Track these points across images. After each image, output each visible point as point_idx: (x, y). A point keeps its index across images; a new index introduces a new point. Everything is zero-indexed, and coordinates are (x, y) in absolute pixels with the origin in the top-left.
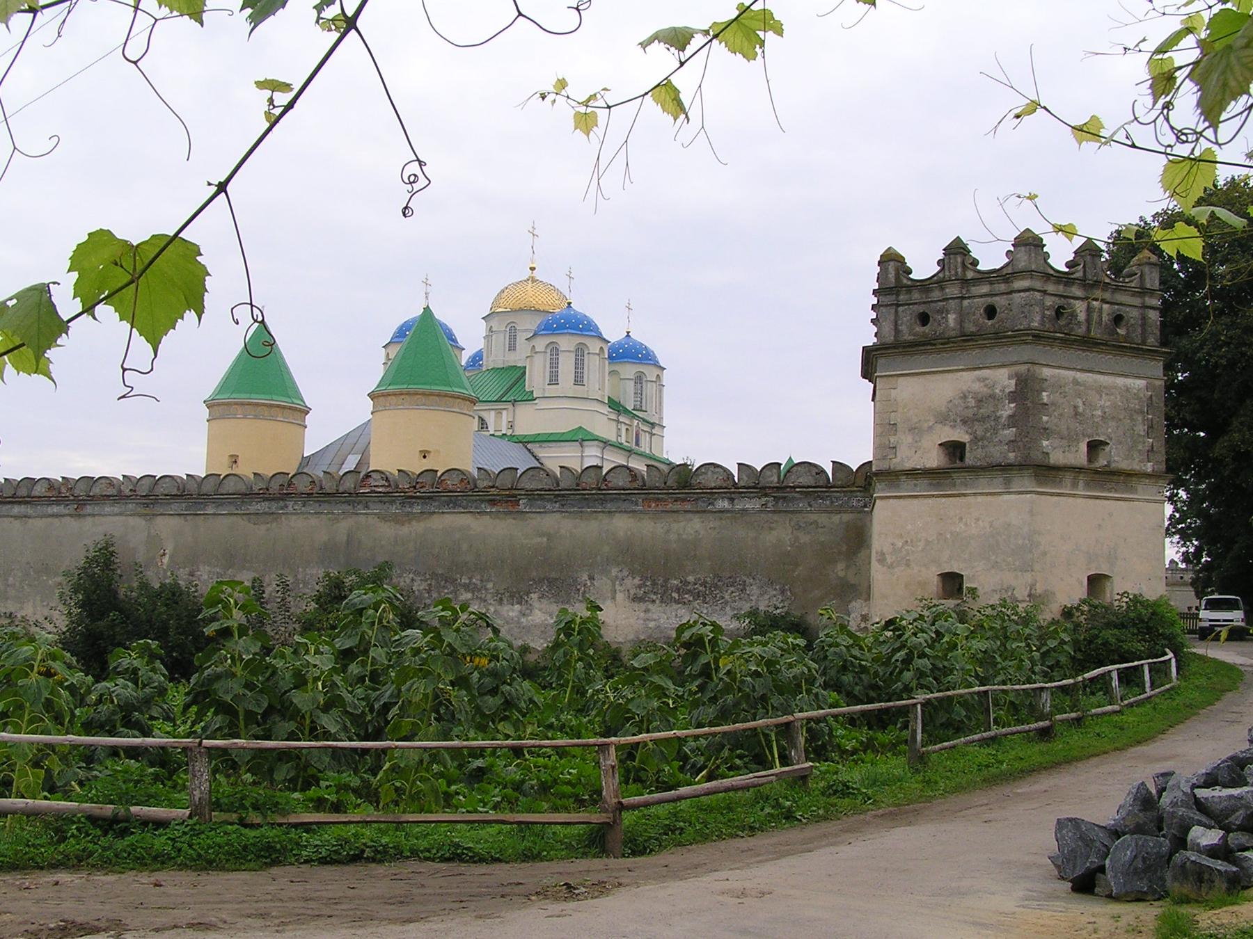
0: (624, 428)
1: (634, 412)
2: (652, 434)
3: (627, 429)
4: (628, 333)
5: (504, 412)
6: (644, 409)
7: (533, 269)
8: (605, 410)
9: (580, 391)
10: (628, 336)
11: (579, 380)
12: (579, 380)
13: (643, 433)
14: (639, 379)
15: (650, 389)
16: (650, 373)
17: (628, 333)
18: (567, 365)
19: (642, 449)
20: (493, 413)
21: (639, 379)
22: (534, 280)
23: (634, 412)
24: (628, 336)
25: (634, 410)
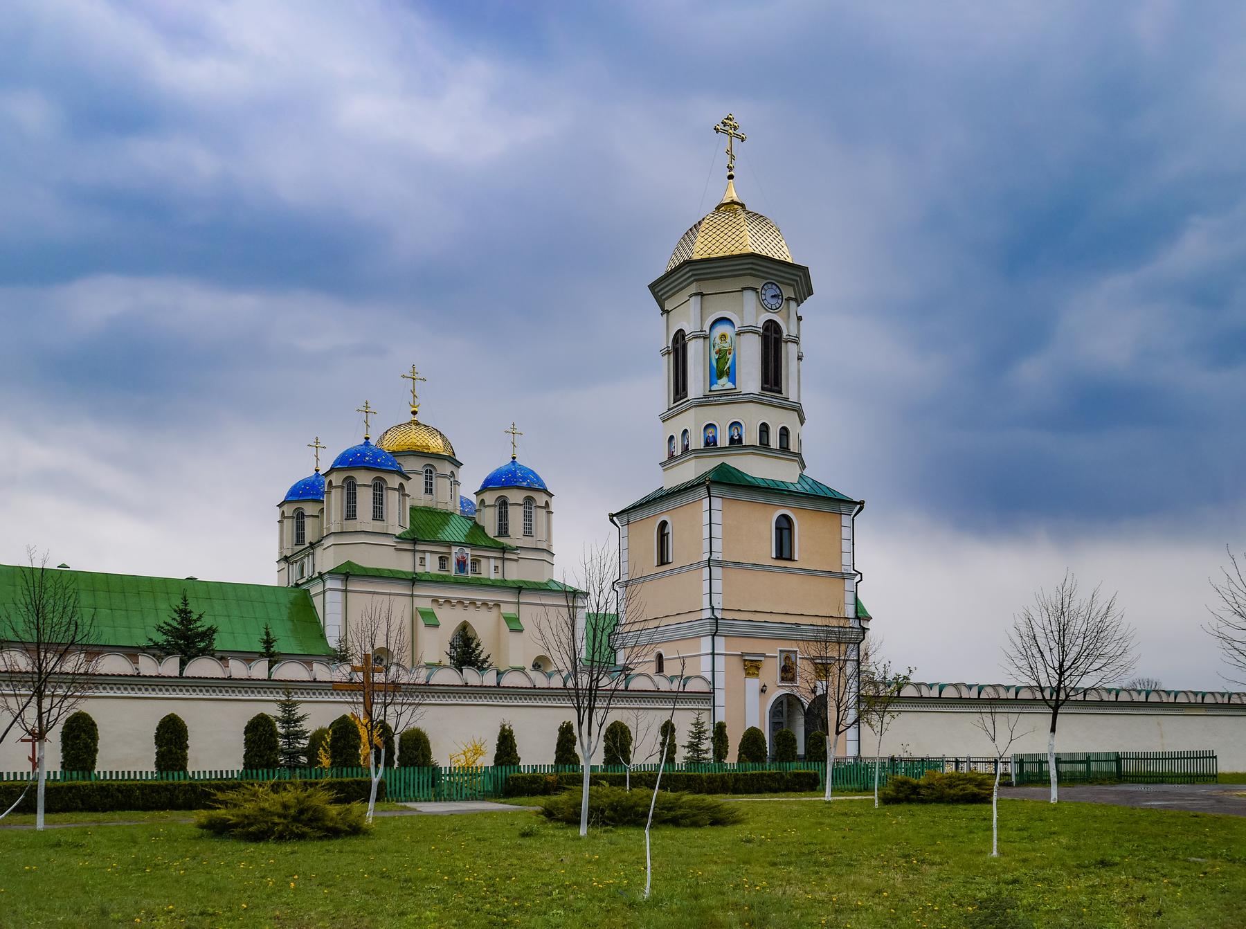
2: (503, 559)
3: (443, 560)
8: (390, 541)
12: (351, 514)
19: (484, 575)
21: (503, 504)
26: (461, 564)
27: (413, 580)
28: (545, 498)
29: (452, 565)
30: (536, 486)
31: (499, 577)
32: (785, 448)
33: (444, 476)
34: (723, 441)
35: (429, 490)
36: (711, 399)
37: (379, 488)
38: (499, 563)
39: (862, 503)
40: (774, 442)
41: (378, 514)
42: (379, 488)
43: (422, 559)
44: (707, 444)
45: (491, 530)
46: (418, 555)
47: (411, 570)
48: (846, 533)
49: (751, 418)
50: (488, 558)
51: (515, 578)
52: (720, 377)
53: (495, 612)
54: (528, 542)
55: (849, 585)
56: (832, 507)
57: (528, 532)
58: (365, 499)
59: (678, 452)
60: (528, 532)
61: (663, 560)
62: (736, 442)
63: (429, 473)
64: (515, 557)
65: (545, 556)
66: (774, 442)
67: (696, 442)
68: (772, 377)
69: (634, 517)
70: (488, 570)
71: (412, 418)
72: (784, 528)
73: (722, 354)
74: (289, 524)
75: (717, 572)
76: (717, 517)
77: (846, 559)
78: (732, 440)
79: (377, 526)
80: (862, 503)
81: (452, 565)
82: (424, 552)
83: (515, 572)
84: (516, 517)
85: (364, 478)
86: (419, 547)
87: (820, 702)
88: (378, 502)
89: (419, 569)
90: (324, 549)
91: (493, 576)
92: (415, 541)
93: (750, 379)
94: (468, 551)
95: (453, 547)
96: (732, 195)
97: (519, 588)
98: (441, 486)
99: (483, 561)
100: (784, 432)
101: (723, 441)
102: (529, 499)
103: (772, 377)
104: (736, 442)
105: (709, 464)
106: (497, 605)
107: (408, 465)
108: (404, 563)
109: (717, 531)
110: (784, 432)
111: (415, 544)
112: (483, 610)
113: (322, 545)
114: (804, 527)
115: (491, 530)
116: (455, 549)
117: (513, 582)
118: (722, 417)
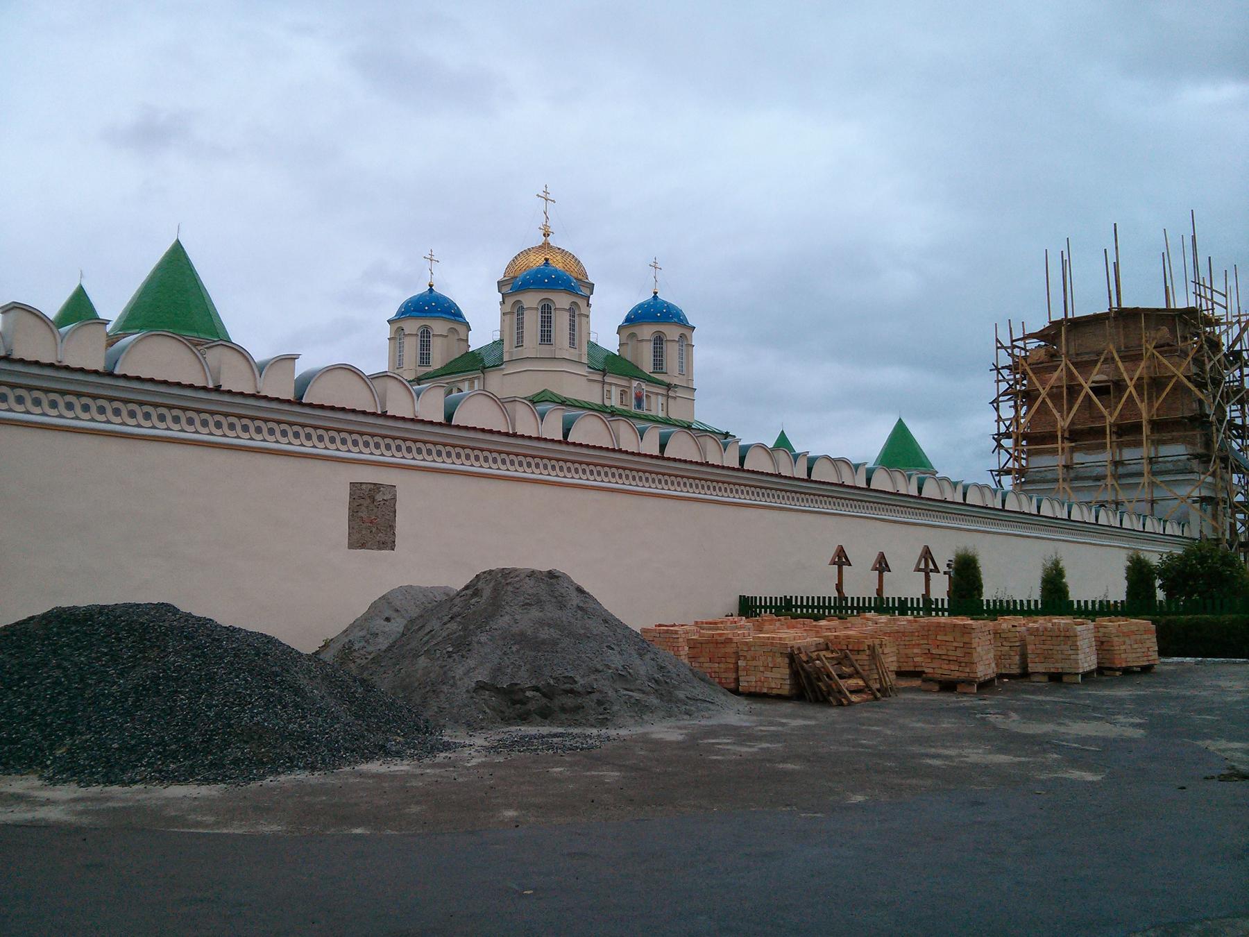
0: (615, 392)
1: (651, 375)
3: (623, 393)
4: (656, 293)
5: (476, 382)
6: (664, 370)
7: (546, 235)
8: (584, 371)
9: (545, 351)
10: (655, 297)
12: (546, 337)
13: (653, 397)
14: (659, 341)
15: (671, 351)
16: (671, 332)
17: (656, 293)
18: (532, 322)
20: (467, 384)
21: (659, 341)
22: (546, 246)
23: (652, 375)
25: (653, 372)
26: (639, 399)
47: (600, 403)
50: (657, 394)
70: (656, 407)
82: (611, 384)
86: (607, 379)
89: (607, 403)
90: (504, 375)
92: (604, 372)
95: (633, 381)
99: (653, 397)
108: (593, 395)
111: (604, 376)
113: (502, 369)
116: (635, 383)
117: (675, 420)
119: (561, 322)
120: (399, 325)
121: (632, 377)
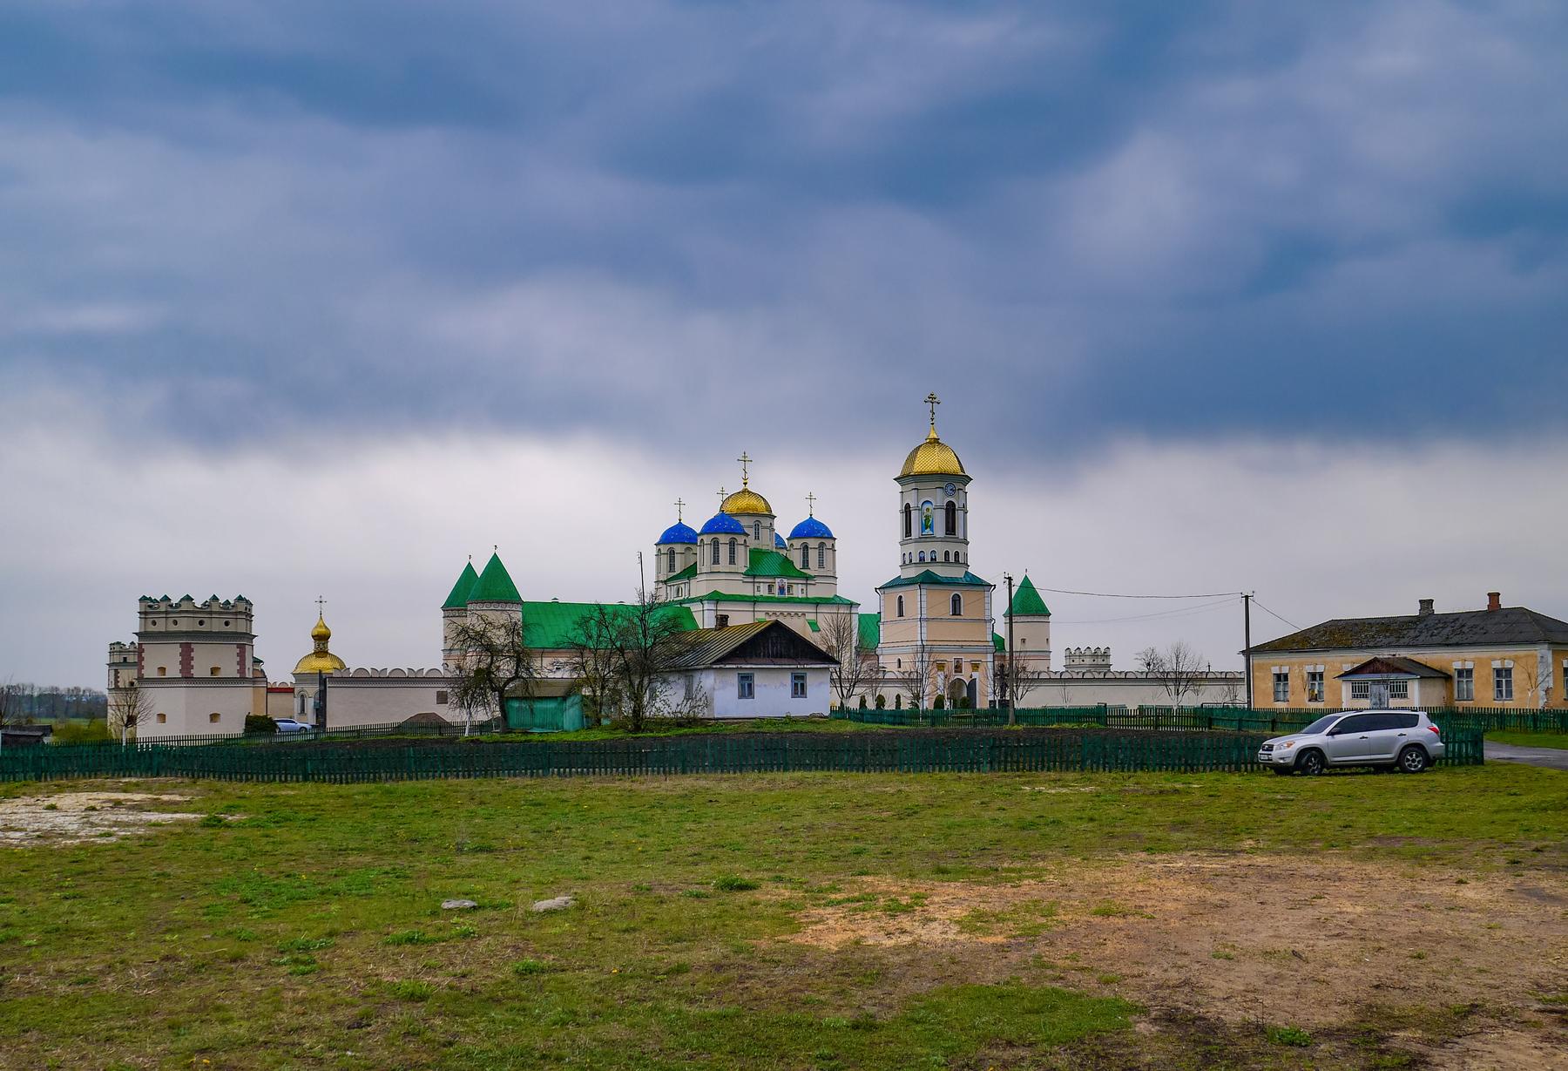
2: (807, 584)
3: (770, 588)
7: (745, 484)
8: (740, 577)
11: (716, 561)
12: (716, 561)
21: (806, 548)
22: (745, 491)
24: (811, 518)
26: (782, 590)
27: (754, 601)
28: (831, 541)
29: (776, 590)
30: (826, 535)
31: (804, 596)
32: (957, 561)
33: (766, 528)
34: (928, 559)
35: (757, 538)
36: (923, 539)
37: (732, 544)
38: (804, 587)
39: (995, 586)
40: (952, 559)
41: (732, 561)
42: (732, 544)
43: (758, 587)
44: (920, 560)
45: (798, 565)
46: (756, 585)
48: (987, 600)
49: (940, 549)
51: (814, 596)
52: (926, 528)
53: (802, 618)
54: (822, 572)
55: (989, 625)
56: (981, 588)
57: (821, 565)
58: (724, 552)
59: (907, 562)
60: (821, 565)
61: (901, 615)
62: (933, 560)
63: (757, 527)
64: (813, 582)
65: (832, 581)
66: (952, 559)
67: (916, 559)
68: (951, 528)
69: (887, 591)
70: (797, 592)
71: (742, 487)
72: (956, 601)
73: (927, 518)
74: (665, 559)
75: (924, 624)
76: (924, 598)
77: (987, 613)
78: (932, 559)
79: (733, 568)
80: (995, 586)
81: (776, 590)
83: (813, 592)
84: (813, 556)
85: (724, 539)
86: (756, 580)
87: (973, 682)
88: (732, 552)
89: (757, 594)
91: (800, 597)
92: (754, 577)
93: (939, 529)
94: (785, 580)
96: (933, 435)
97: (817, 602)
98: (764, 533)
100: (957, 554)
101: (928, 559)
102: (822, 545)
103: (951, 528)
104: (933, 560)
105: (922, 570)
106: (804, 614)
107: (745, 522)
108: (747, 590)
109: (924, 605)
110: (957, 554)
111: (754, 578)
112: (796, 618)
114: (967, 598)
115: (798, 565)
116: (778, 580)
117: (812, 599)
118: (927, 548)
119: (724, 552)
120: (659, 547)
121: (774, 577)
